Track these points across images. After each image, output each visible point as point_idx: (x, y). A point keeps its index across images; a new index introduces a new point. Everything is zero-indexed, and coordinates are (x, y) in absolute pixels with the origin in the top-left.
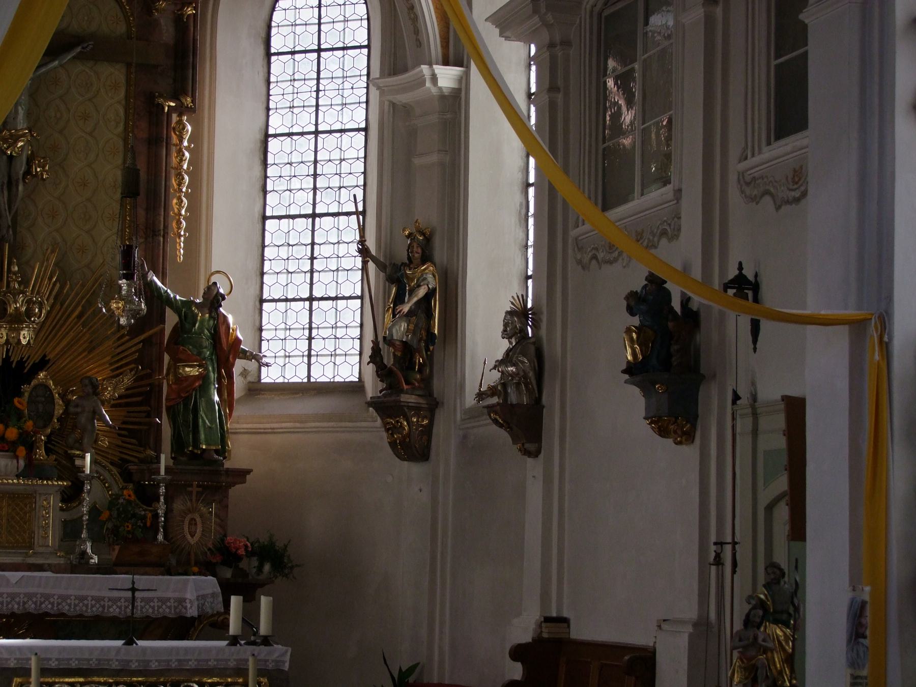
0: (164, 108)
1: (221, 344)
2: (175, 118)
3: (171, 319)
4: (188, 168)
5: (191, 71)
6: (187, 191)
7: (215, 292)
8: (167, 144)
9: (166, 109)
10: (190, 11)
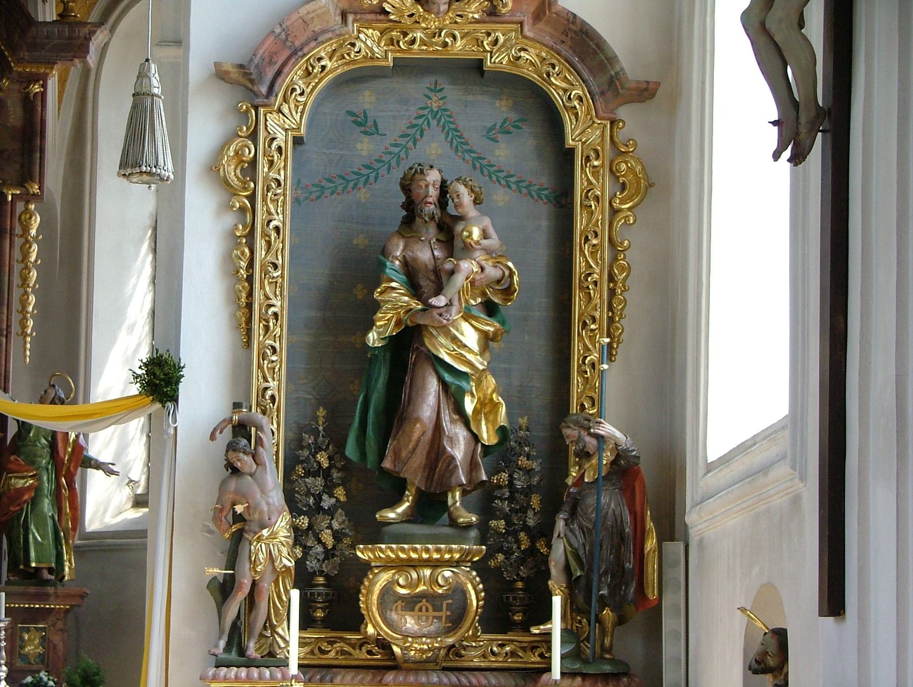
0: (6, 197)
1: (58, 453)
2: (20, 206)
3: (12, 430)
4: (36, 261)
5: (38, 155)
6: (34, 286)
7: (53, 396)
8: (11, 235)
9: (10, 198)
10: (37, 88)
